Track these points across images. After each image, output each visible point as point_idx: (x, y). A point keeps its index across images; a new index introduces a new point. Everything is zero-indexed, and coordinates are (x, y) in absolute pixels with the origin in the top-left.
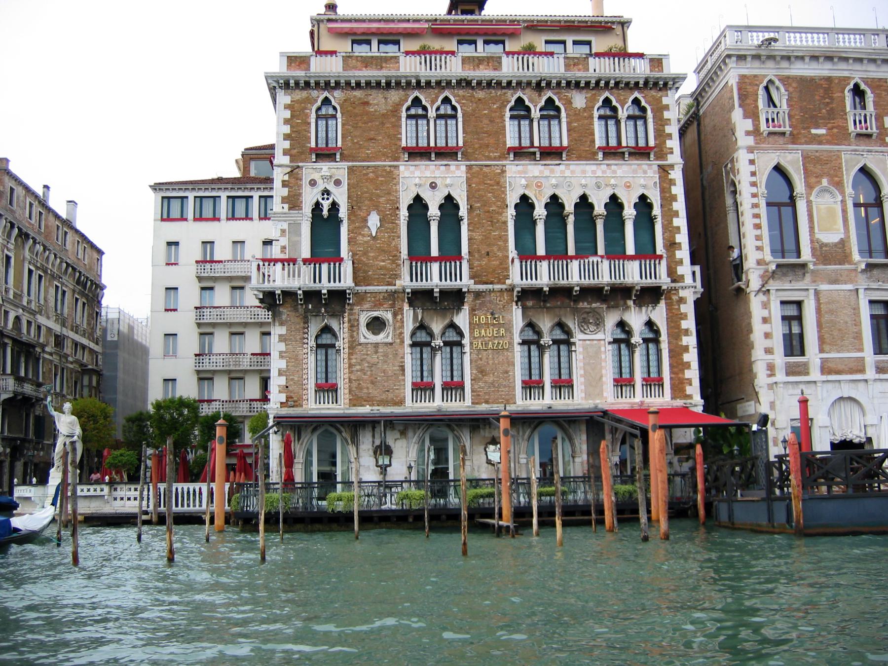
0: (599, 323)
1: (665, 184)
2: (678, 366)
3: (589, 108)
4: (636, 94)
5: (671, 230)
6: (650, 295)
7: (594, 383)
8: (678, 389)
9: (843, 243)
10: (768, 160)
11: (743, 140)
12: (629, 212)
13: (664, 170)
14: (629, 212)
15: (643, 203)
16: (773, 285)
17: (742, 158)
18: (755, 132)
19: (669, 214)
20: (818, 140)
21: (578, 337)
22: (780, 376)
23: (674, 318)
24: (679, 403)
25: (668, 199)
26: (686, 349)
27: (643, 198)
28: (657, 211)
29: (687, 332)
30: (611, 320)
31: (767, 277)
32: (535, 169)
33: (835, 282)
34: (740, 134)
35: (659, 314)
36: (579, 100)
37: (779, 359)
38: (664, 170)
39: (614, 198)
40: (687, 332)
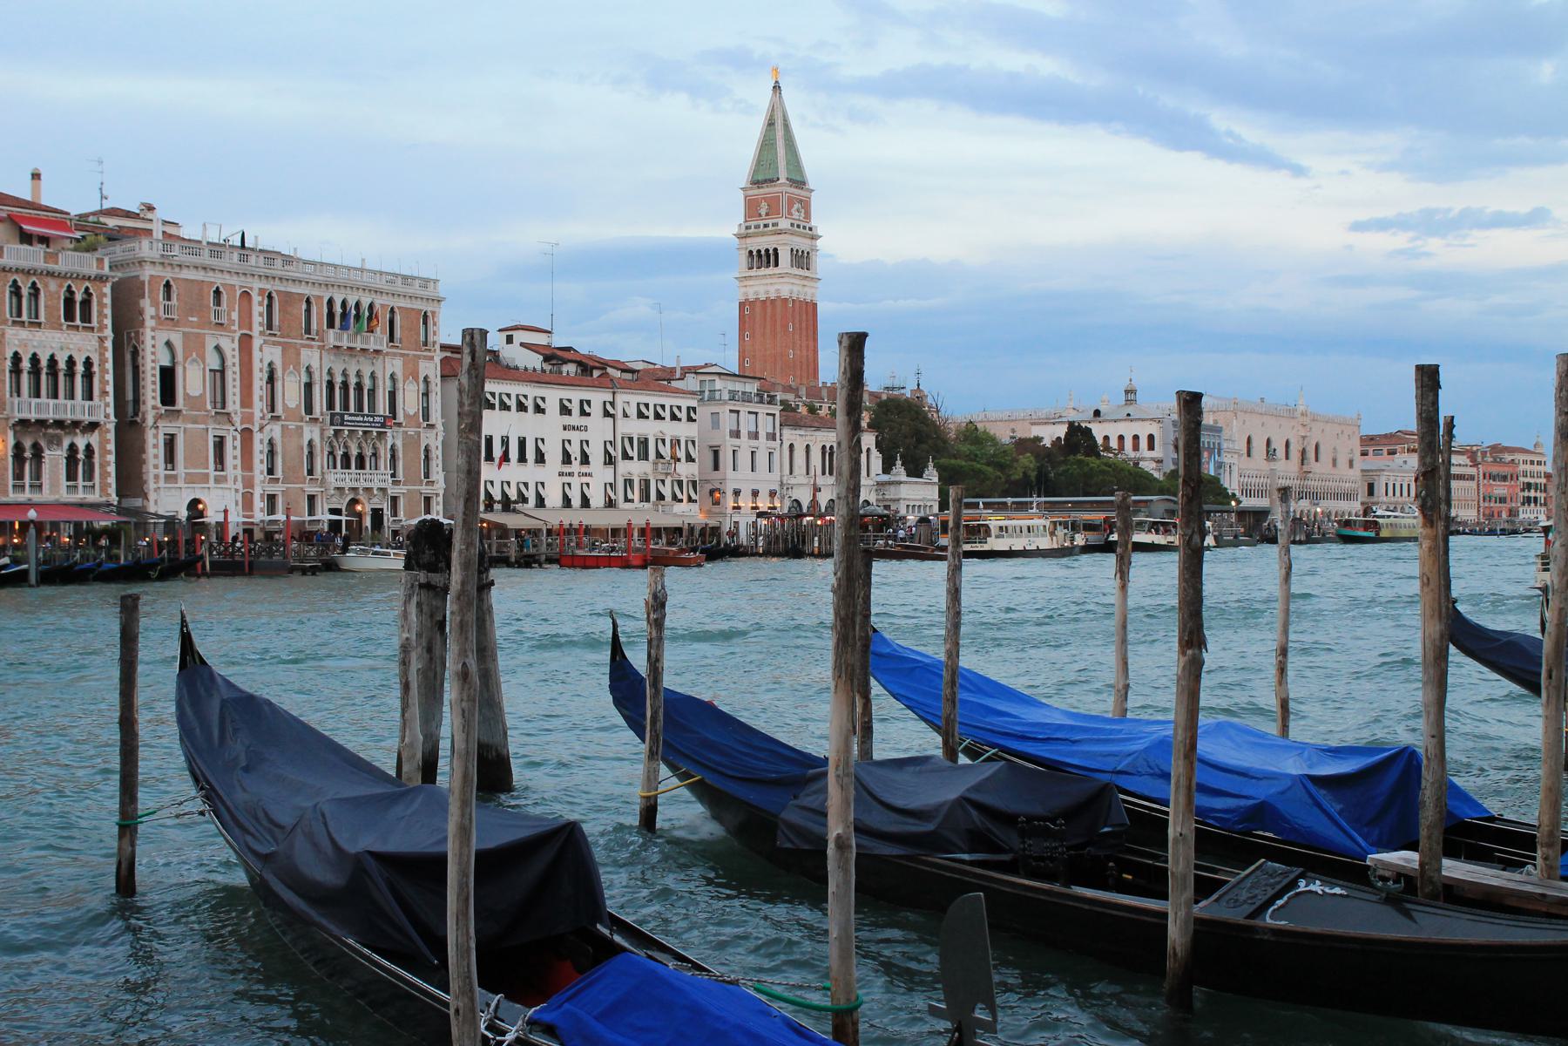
0: (59, 444)
1: (103, 349)
2: (105, 475)
3: (58, 293)
4: (87, 284)
5: (103, 382)
6: (93, 426)
7: (54, 486)
8: (104, 489)
9: (203, 396)
10: (163, 336)
11: (149, 323)
12: (80, 368)
13: (102, 340)
14: (80, 368)
15: (88, 363)
16: (160, 424)
17: (148, 334)
18: (156, 317)
19: (104, 371)
20: (191, 324)
21: (47, 453)
22: (162, 484)
23: (103, 442)
24: (104, 499)
25: (103, 361)
26: (108, 463)
27: (88, 358)
28: (96, 368)
29: (109, 452)
30: (66, 443)
31: (158, 417)
32: (24, 334)
33: (195, 422)
34: (147, 317)
35: (94, 439)
36: (53, 285)
37: (162, 472)
38: (102, 340)
39: (71, 357)
40: (109, 452)
